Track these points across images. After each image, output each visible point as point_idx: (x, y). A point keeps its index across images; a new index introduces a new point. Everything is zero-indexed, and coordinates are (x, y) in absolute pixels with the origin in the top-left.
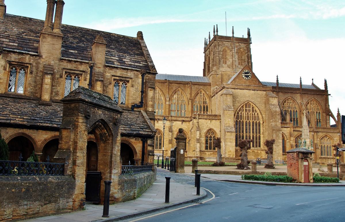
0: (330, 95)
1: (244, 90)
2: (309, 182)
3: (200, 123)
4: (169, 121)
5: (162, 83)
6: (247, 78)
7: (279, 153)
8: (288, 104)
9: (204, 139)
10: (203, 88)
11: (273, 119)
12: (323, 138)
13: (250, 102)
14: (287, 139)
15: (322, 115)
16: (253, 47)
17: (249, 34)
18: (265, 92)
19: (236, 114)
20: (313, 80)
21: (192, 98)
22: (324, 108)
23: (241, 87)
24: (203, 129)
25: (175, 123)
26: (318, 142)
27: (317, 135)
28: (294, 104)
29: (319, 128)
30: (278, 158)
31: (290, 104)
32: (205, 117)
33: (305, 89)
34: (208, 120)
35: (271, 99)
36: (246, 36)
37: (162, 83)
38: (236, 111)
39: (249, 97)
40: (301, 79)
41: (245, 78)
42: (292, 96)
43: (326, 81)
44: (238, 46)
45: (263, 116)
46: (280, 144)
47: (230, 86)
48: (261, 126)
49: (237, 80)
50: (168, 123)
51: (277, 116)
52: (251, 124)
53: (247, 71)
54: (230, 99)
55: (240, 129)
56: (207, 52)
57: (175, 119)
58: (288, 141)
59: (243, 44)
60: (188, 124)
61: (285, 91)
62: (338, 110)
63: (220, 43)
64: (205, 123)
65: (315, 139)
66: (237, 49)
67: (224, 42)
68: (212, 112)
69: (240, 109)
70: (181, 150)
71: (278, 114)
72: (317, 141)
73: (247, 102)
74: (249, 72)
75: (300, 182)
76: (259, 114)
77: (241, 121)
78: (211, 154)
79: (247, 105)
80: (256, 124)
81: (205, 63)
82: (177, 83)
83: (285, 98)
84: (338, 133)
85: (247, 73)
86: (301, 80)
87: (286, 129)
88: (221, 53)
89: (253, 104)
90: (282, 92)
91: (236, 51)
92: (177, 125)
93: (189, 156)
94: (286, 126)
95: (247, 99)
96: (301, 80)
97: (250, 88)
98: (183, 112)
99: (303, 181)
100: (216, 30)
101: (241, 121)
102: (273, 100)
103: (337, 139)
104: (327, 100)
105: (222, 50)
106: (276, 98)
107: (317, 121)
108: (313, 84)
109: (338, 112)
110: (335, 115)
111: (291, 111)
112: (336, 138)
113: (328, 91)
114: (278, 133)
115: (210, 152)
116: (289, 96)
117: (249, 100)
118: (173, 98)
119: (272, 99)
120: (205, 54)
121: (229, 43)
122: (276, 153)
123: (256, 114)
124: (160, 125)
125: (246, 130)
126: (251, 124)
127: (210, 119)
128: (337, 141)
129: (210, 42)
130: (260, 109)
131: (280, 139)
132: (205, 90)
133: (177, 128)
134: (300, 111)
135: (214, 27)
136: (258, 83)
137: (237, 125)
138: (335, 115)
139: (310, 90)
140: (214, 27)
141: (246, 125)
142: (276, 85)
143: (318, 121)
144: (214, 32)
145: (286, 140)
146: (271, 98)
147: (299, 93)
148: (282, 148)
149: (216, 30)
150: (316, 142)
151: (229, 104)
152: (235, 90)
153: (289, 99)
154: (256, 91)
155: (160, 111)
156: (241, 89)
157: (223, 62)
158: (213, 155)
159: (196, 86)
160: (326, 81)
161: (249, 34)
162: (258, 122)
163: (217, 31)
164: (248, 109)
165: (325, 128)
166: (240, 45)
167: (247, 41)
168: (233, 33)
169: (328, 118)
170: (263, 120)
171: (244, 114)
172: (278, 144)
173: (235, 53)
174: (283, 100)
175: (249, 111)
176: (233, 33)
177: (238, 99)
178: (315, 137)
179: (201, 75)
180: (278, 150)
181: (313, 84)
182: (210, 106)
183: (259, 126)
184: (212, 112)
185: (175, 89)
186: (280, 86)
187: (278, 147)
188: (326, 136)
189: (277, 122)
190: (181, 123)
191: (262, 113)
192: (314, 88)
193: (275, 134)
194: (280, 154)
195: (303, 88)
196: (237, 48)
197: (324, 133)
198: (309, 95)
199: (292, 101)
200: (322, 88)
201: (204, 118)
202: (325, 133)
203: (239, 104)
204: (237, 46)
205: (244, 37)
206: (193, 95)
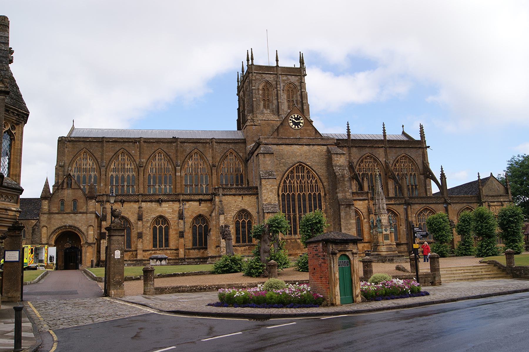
0: (429, 147)
2: (353, 301)
3: (224, 202)
4: (179, 201)
5: (168, 142)
6: (296, 127)
8: (367, 165)
9: (233, 228)
10: (233, 148)
12: (421, 212)
14: (364, 219)
15: (419, 178)
16: (309, 80)
17: (302, 62)
18: (325, 147)
19: (282, 184)
20: (403, 126)
21: (217, 164)
22: (421, 167)
23: (288, 141)
24: (230, 211)
25: (188, 205)
26: (414, 219)
27: (411, 209)
28: (376, 165)
29: (414, 198)
32: (233, 192)
33: (392, 141)
34: (237, 197)
35: (334, 157)
36: (298, 65)
37: (168, 142)
38: (282, 179)
40: (384, 125)
41: (294, 126)
43: (421, 127)
44: (286, 80)
45: (325, 184)
47: (270, 141)
48: (323, 200)
49: (281, 130)
50: (176, 206)
52: (307, 198)
53: (296, 116)
54: (270, 160)
55: (289, 207)
56: (241, 93)
57: (187, 197)
58: (365, 220)
60: (209, 205)
61: (361, 145)
62: (442, 169)
63: (257, 77)
64: (234, 202)
65: (409, 215)
66: (284, 84)
67: (264, 75)
68: (248, 184)
69: (288, 175)
70: (116, 252)
72: (413, 218)
74: (300, 117)
75: (333, 305)
76: (319, 181)
77: (291, 194)
78: (244, 250)
79: (301, 167)
80: (315, 199)
81: (239, 109)
82: (192, 143)
84: (443, 203)
85: (297, 119)
86: (384, 128)
88: (261, 92)
90: (356, 147)
91: (282, 88)
92: (193, 208)
93: (210, 255)
94: (361, 198)
95: (298, 160)
96: (384, 128)
97: (301, 142)
98: (204, 186)
99: (338, 300)
100: (250, 58)
101: (291, 194)
104: (424, 156)
105: (261, 88)
106: (342, 155)
107: (412, 188)
108: (403, 133)
109: (442, 171)
110: (438, 178)
113: (425, 141)
114: (348, 209)
115: (244, 248)
116: (367, 152)
117: (301, 161)
118: (186, 166)
120: (239, 96)
121: (272, 76)
123: (314, 181)
124: (164, 209)
125: (300, 207)
126: (307, 198)
127: (240, 195)
129: (243, 77)
130: (319, 174)
132: (236, 150)
133: (199, 211)
134: (386, 174)
135: (248, 54)
136: (314, 133)
137: (285, 201)
138: (438, 178)
139: (398, 141)
140: (248, 54)
141: (299, 201)
142: (346, 137)
143: (414, 187)
144: (248, 60)
146: (336, 156)
147: (382, 147)
149: (250, 58)
150: (410, 219)
151: (269, 168)
153: (368, 156)
154: (311, 146)
155: (168, 187)
156: (288, 144)
157: (264, 106)
158: (249, 251)
159: (222, 145)
160: (421, 127)
161: (302, 62)
162: (317, 194)
163: (252, 59)
164: (300, 175)
165: (424, 198)
166: (288, 79)
167: (299, 72)
168: (277, 61)
169: (427, 183)
170: (325, 191)
171: (296, 183)
173: (282, 91)
175: (303, 177)
176: (277, 61)
178: (409, 212)
179: (234, 127)
181: (403, 133)
182: (245, 174)
183: (320, 200)
184: (248, 184)
185: (190, 151)
186: (352, 137)
188: (426, 209)
189: (346, 192)
190: (197, 203)
191: (323, 180)
192: (405, 139)
195: (387, 139)
196: (284, 82)
199: (372, 160)
200: (417, 137)
201: (231, 193)
202: (424, 205)
203: (286, 169)
205: (296, 67)
206: (218, 159)
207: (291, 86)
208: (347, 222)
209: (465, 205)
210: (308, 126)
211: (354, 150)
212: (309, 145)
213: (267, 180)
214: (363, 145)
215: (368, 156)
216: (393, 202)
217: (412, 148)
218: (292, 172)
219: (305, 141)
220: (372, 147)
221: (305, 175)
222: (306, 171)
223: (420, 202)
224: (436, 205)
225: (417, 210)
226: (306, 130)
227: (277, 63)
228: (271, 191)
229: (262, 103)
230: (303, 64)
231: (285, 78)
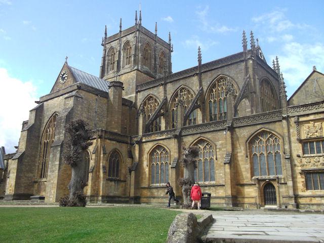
7: (53, 183)
17: (138, 18)
59: (131, 35)
90: (171, 82)
103: (222, 144)
112: (220, 142)
121: (116, 41)
128: (223, 148)
168: (121, 27)
172: (54, 169)
176: (121, 27)
197: (195, 135)
198: (213, 72)
209: (259, 127)
216: (164, 137)
217: (231, 64)
220: (186, 78)
223: (195, 132)
224: (214, 134)
225: (189, 143)
227: (121, 29)
230: (140, 20)
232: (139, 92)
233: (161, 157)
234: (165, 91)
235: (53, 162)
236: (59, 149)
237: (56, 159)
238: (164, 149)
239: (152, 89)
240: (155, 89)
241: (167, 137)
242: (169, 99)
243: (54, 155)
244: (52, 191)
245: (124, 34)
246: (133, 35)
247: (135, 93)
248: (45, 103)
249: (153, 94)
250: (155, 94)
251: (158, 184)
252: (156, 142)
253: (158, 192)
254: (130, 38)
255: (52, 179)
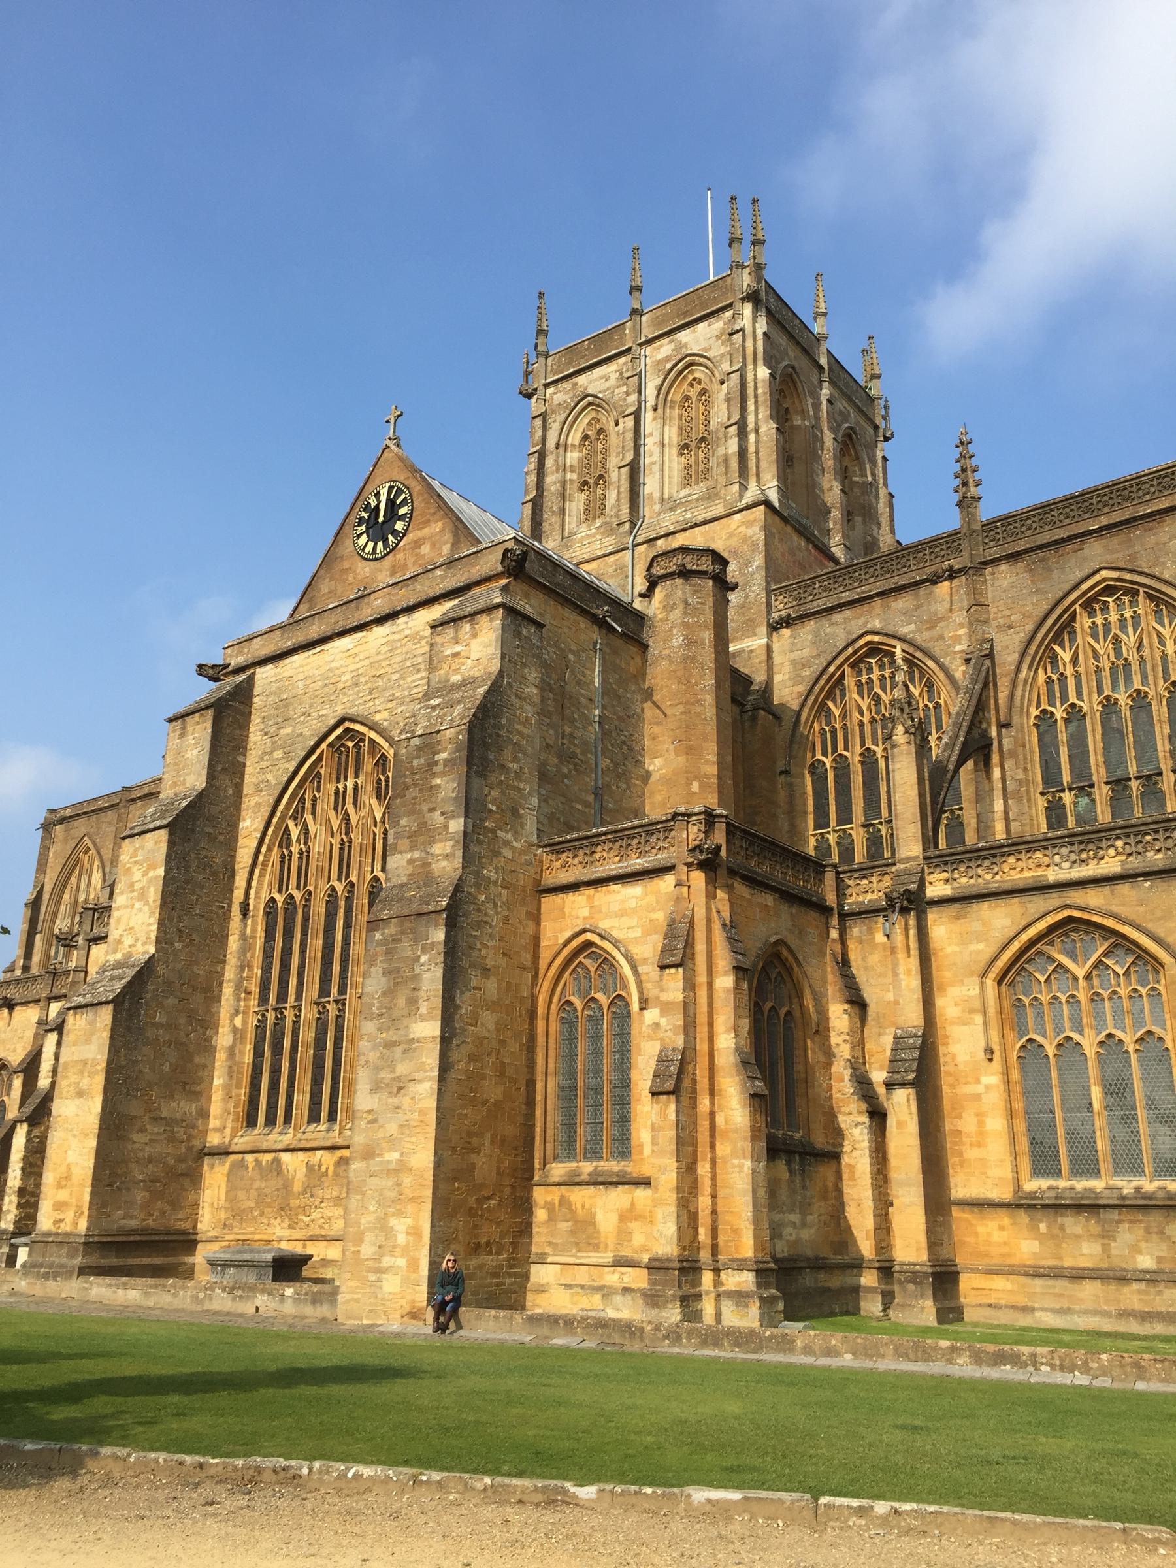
1: (328, 646)
6: (380, 545)
7: (402, 1168)
11: (403, 822)
13: (358, 727)
30: (393, 1221)
31: (1129, 639)
39: (356, 685)
42: (1133, 557)
46: (421, 1068)
51: (438, 781)
59: (701, 326)
67: (582, 379)
71: (446, 761)
73: (339, 731)
83: (1052, 597)
87: (633, 892)
88: (573, 457)
89: (373, 735)
90: (1014, 557)
91: (651, 402)
102: (458, 648)
105: (575, 438)
106: (483, 620)
111: (1140, 701)
114: (406, 948)
119: (457, 641)
122: (375, 1164)
131: (423, 1010)
145: (635, 1006)
146: (450, 631)
148: (432, 1103)
152: (282, 663)
153: (1109, 590)
154: (402, 620)
166: (680, 346)
172: (402, 1069)
174: (1030, 626)
177: (289, 730)
180: (392, 1128)
187: (395, 1101)
193: (377, 970)
194: (407, 1181)
199: (1143, 607)
204: (660, 362)
207: (699, 373)
208: (391, 1036)
210: (427, 522)
211: (1004, 581)
212: (391, 616)
213: (138, 840)
214: (1062, 534)
215: (1109, 590)
216: (1111, 864)
218: (314, 776)
219: (379, 604)
221: (366, 781)
222: (368, 764)
226: (417, 544)
228: (143, 895)
229: (577, 502)
231: (664, 349)
232: (787, 622)
233: (1095, 998)
234: (977, 604)
235: (390, 1019)
236: (440, 935)
237: (413, 1002)
238: (1120, 943)
239: (877, 603)
240: (903, 603)
241: (1135, 864)
242: (1007, 658)
243: (401, 978)
244: (400, 1226)
245: (656, 323)
246: (717, 325)
247: (764, 630)
248: (263, 675)
249: (890, 629)
250: (904, 630)
251: (1098, 1185)
252: (1053, 900)
253: (1107, 1236)
254: (700, 338)
255: (393, 1143)
